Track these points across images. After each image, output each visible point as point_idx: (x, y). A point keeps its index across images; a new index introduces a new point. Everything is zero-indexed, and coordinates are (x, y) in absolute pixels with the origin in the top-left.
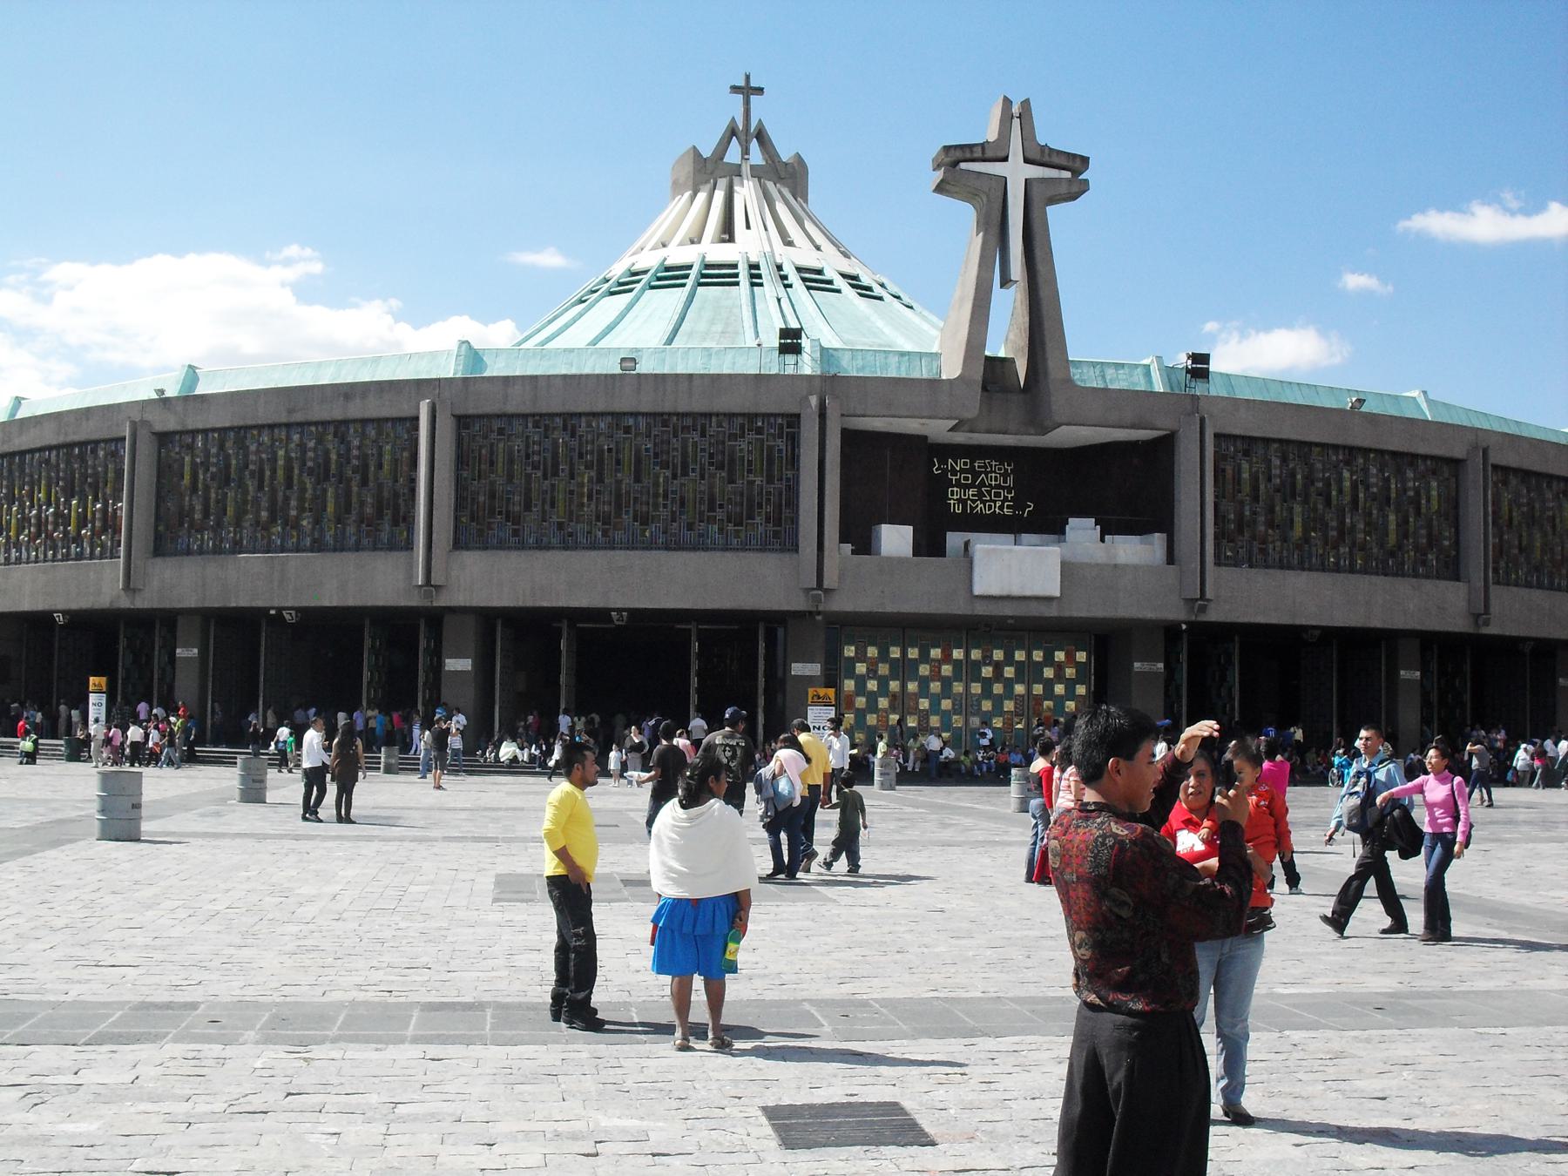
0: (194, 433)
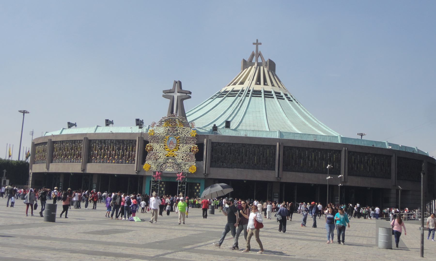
0: (57, 141)
